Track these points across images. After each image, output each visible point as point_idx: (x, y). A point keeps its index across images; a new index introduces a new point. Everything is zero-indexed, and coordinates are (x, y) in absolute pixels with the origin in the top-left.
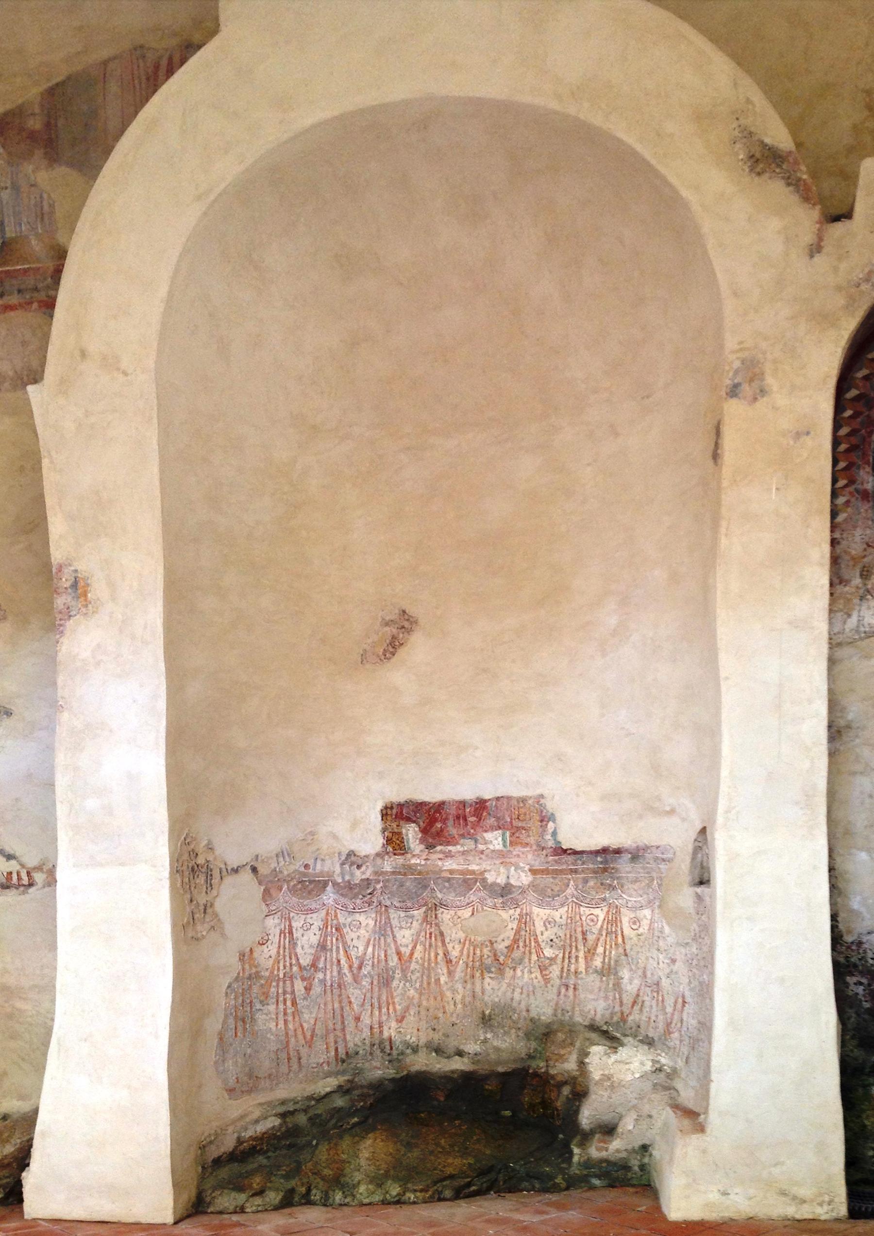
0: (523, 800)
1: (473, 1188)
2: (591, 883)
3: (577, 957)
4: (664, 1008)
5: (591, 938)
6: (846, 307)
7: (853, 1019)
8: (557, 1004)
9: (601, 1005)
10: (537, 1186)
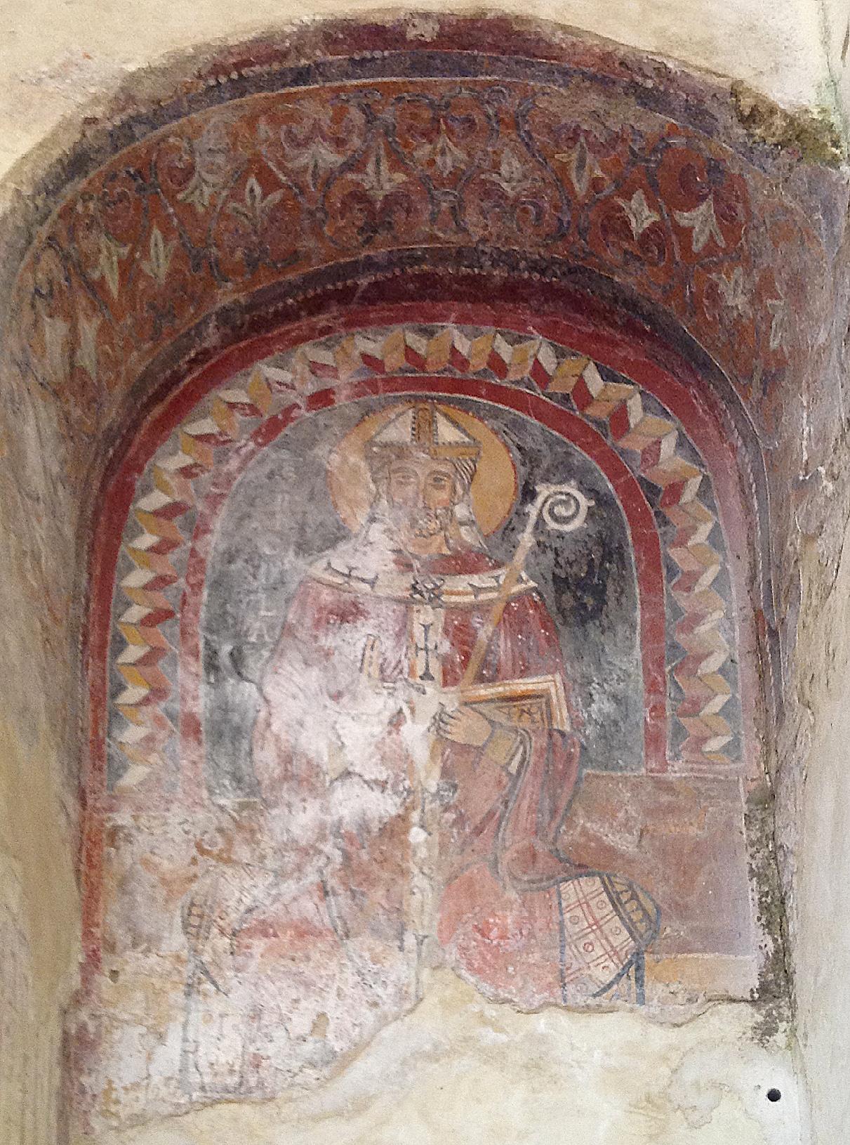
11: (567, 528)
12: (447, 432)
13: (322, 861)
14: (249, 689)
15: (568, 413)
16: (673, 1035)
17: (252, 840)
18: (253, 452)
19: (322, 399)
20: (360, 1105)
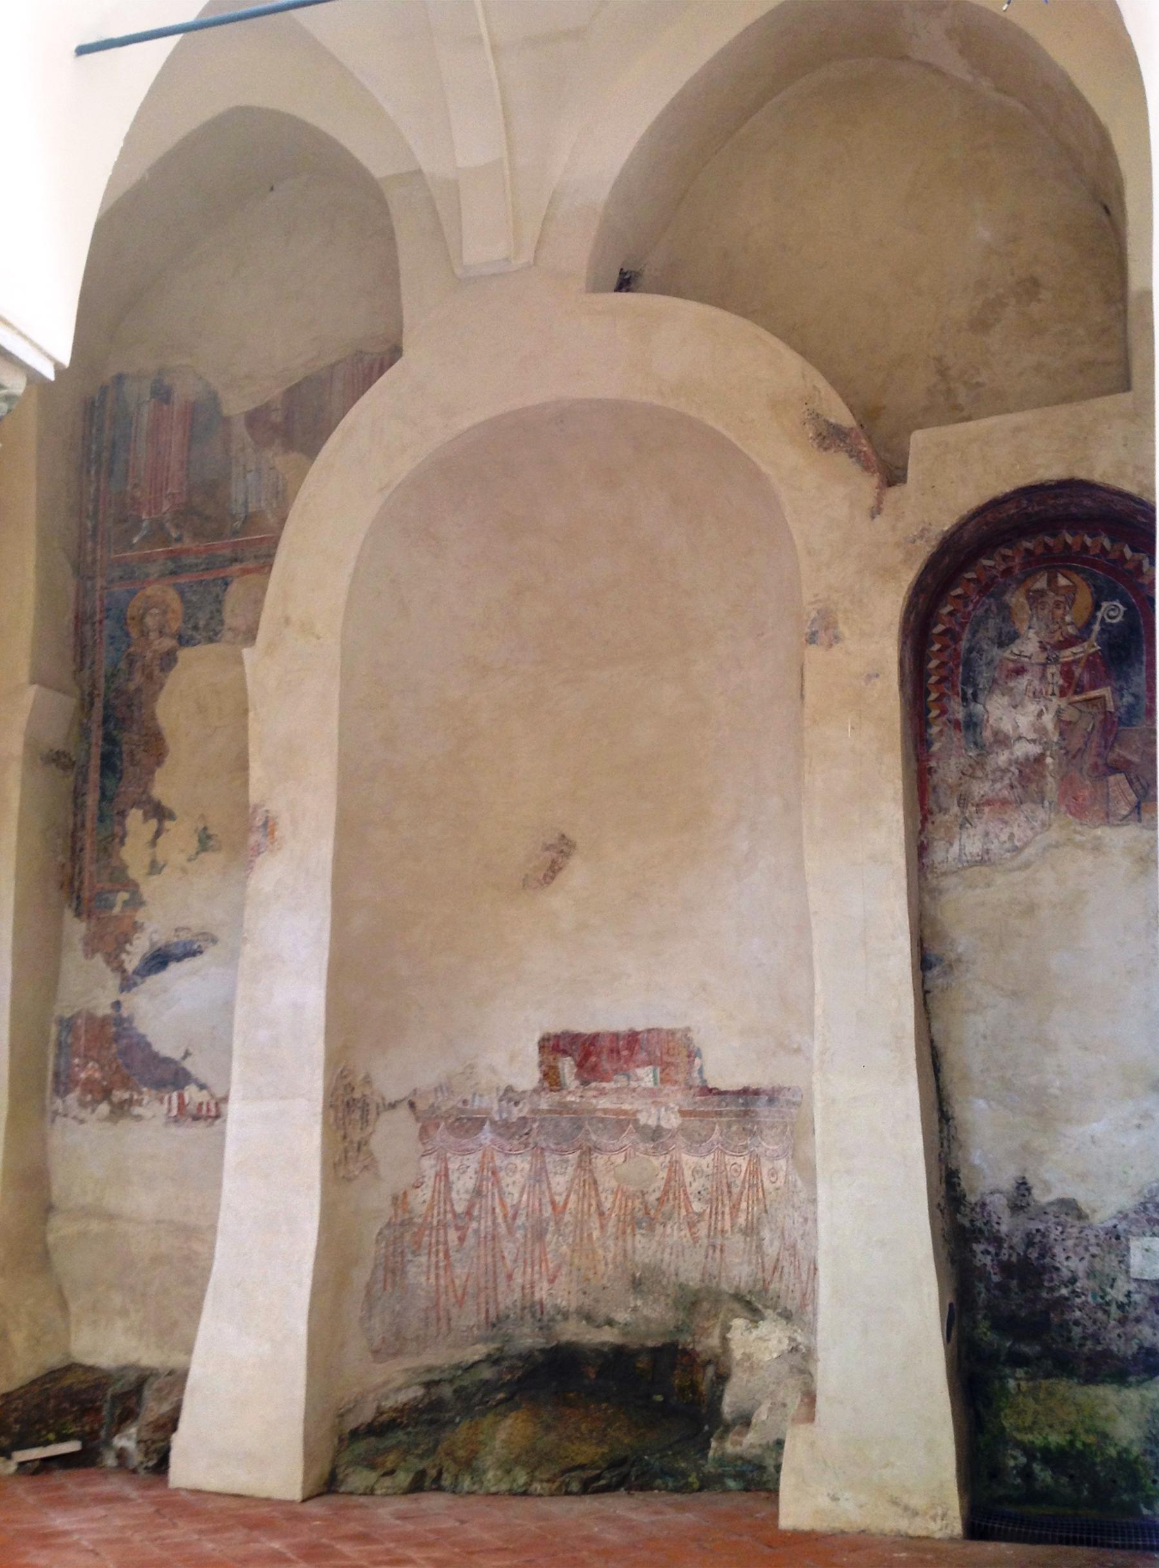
0: (672, 1033)
1: (603, 1482)
2: (734, 1128)
3: (723, 1213)
5: (736, 1190)
8: (704, 1268)
9: (746, 1270)
10: (670, 1485)
11: (1114, 621)
12: (1062, 581)
13: (1010, 775)
14: (979, 707)
19: (1008, 572)
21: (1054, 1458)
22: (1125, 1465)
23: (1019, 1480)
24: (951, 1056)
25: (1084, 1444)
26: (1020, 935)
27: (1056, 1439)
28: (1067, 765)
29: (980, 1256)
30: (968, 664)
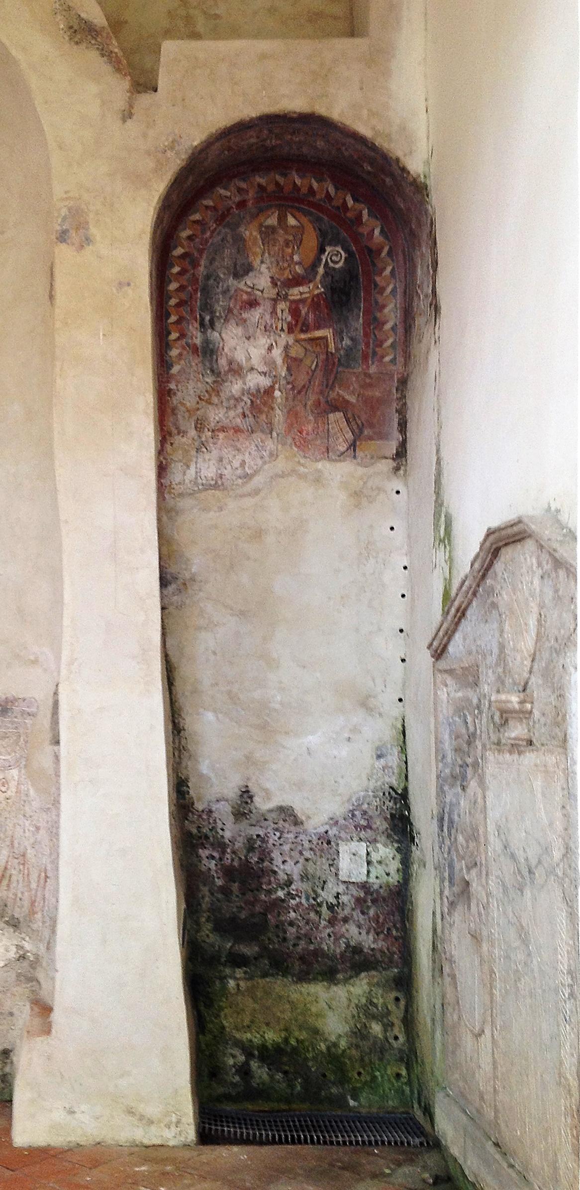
4: (29, 885)
6: (155, 171)
7: (207, 899)
11: (337, 266)
12: (291, 221)
13: (243, 404)
14: (216, 334)
15: (339, 214)
16: (365, 470)
17: (218, 395)
18: (215, 229)
19: (242, 204)
20: (257, 492)
21: (271, 1055)
22: (334, 1058)
23: (237, 1078)
24: (184, 671)
25: (297, 1041)
26: (248, 558)
27: (272, 1036)
28: (294, 400)
29: (205, 861)
30: (206, 290)
